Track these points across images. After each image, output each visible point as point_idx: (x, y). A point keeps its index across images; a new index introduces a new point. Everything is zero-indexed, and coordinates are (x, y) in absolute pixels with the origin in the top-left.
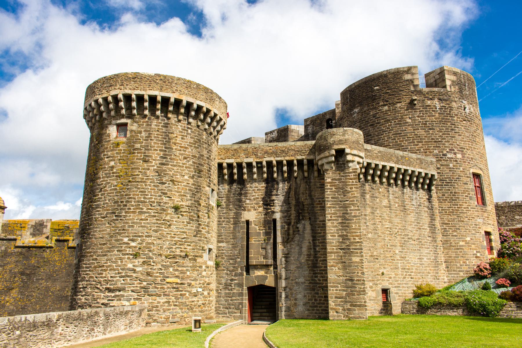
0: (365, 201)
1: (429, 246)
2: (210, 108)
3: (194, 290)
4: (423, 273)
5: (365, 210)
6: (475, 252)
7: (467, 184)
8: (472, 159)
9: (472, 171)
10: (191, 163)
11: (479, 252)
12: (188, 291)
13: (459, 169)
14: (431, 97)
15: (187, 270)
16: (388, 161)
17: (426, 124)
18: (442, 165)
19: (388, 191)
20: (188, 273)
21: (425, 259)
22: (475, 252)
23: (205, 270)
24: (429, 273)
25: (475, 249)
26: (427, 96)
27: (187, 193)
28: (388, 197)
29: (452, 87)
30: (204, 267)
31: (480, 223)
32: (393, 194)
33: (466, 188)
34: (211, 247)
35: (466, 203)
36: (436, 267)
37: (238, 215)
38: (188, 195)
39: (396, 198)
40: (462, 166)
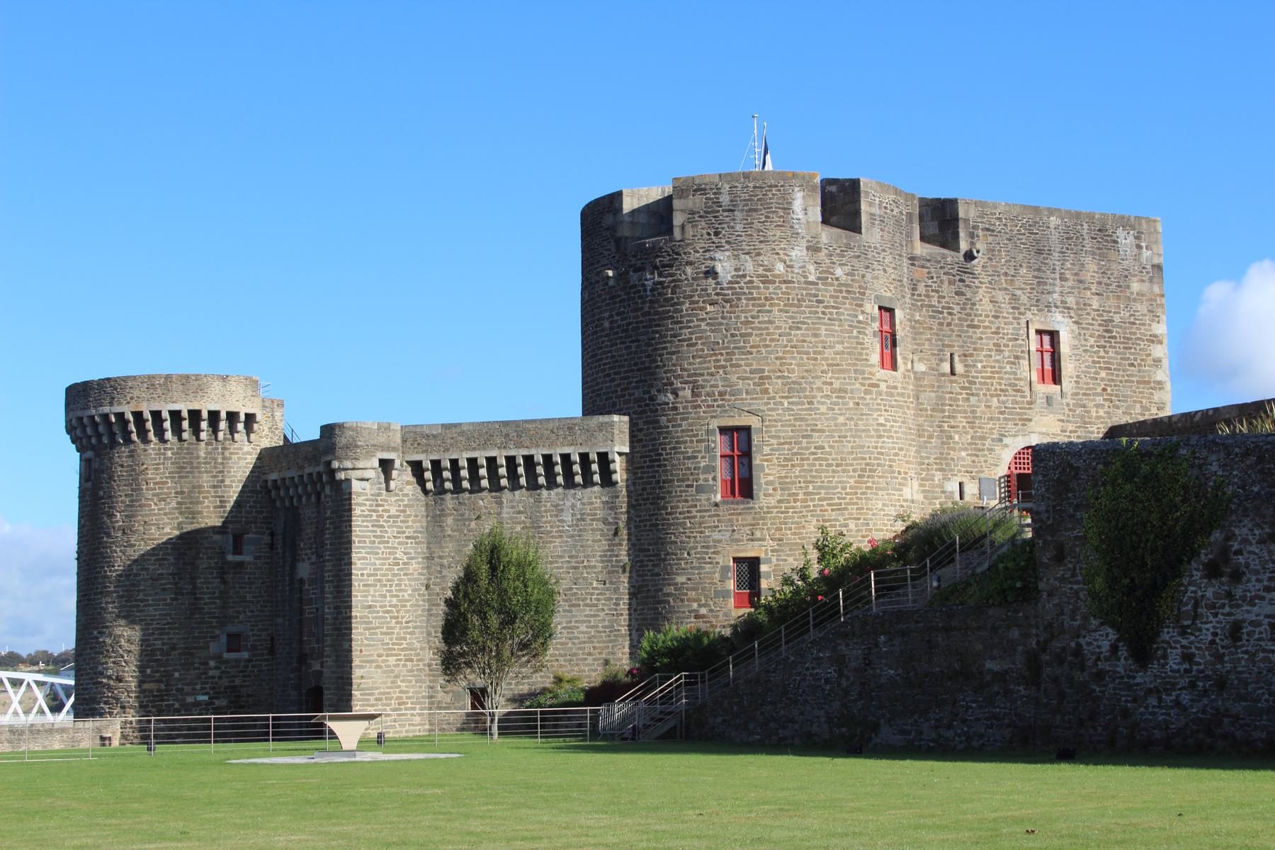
0: (443, 531)
1: (598, 600)
2: (197, 408)
3: (190, 699)
4: (575, 654)
5: (441, 547)
6: (695, 605)
7: (696, 457)
8: (721, 394)
9: (714, 424)
10: (174, 504)
11: (705, 605)
12: (177, 700)
13: (680, 426)
14: (639, 264)
15: (175, 670)
16: (484, 446)
17: (627, 330)
18: (646, 423)
19: (502, 503)
20: (177, 675)
21: (583, 628)
22: (695, 605)
23: (216, 668)
24: (590, 654)
25: (695, 600)
26: (633, 261)
27: (168, 554)
28: (499, 514)
29: (688, 227)
30: (212, 663)
31: (720, 541)
32: (513, 507)
33: (689, 469)
34: (232, 628)
35: (687, 501)
36: (611, 641)
37: (293, 568)
38: (171, 558)
39: (519, 512)
40: (687, 419)
